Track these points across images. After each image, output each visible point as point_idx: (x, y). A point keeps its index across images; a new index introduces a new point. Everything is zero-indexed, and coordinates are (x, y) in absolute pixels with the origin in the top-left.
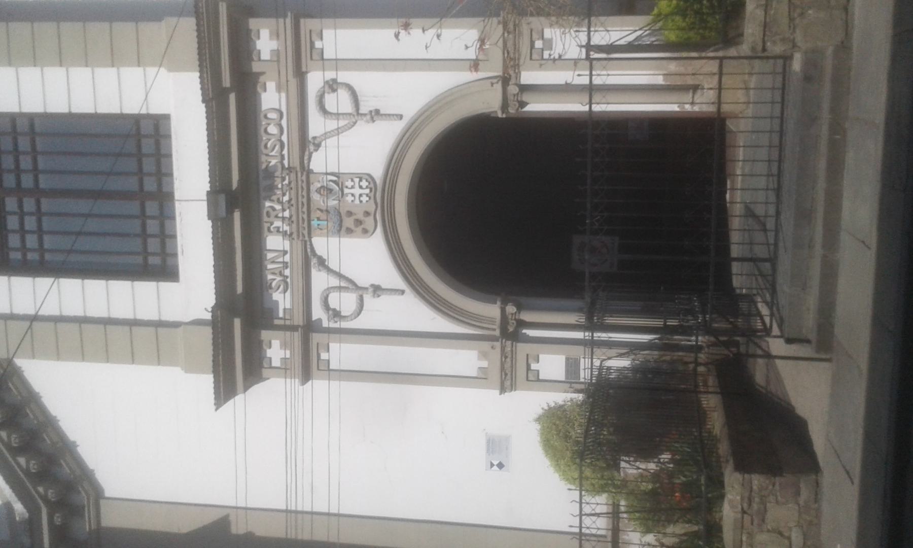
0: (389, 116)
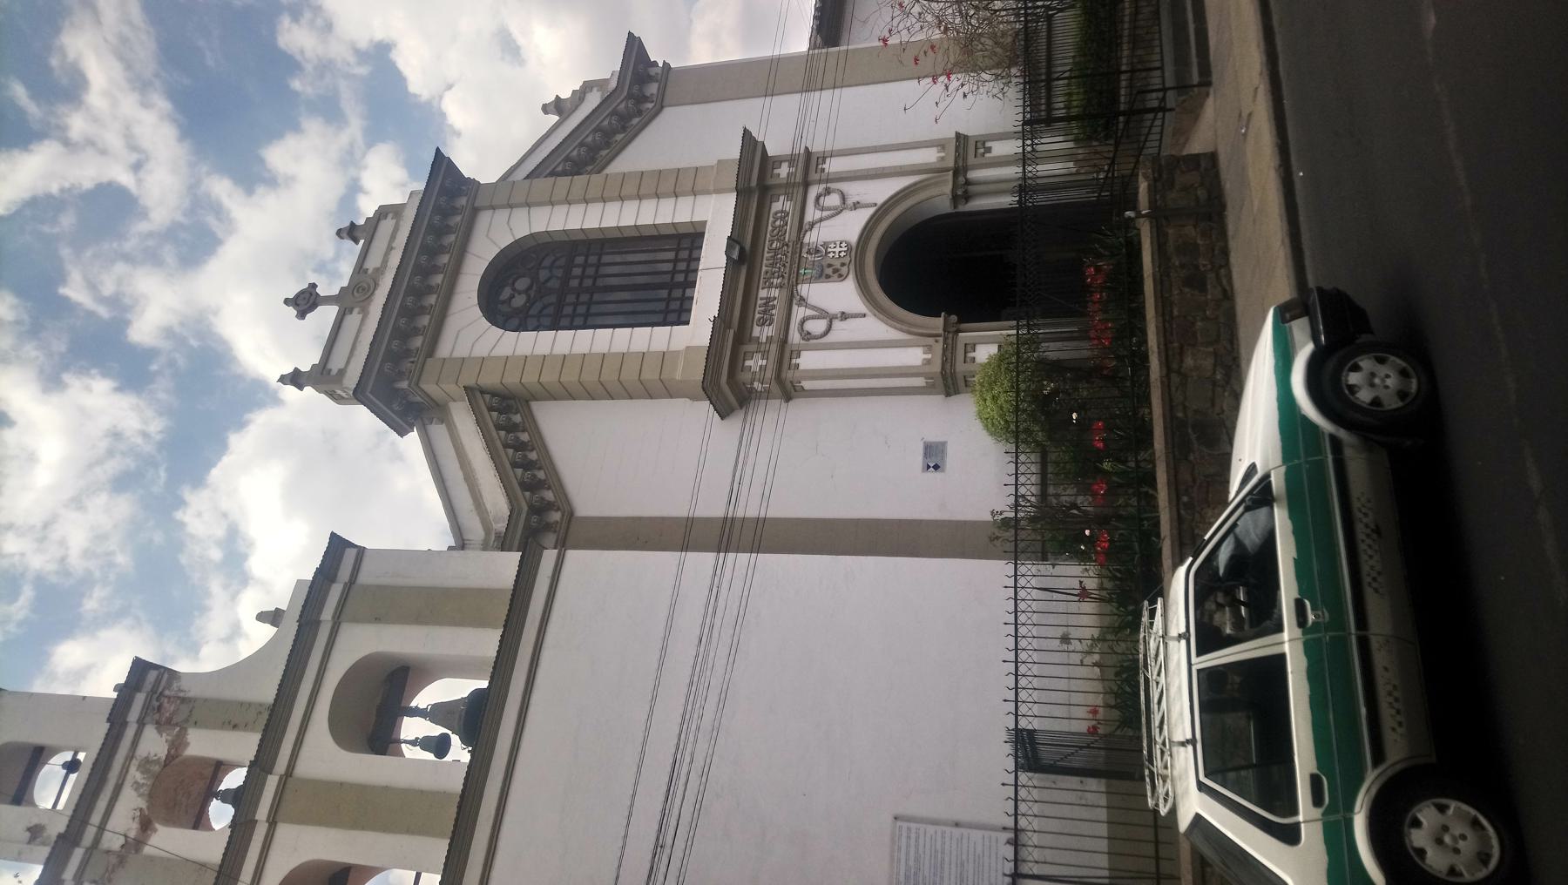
0: (867, 206)
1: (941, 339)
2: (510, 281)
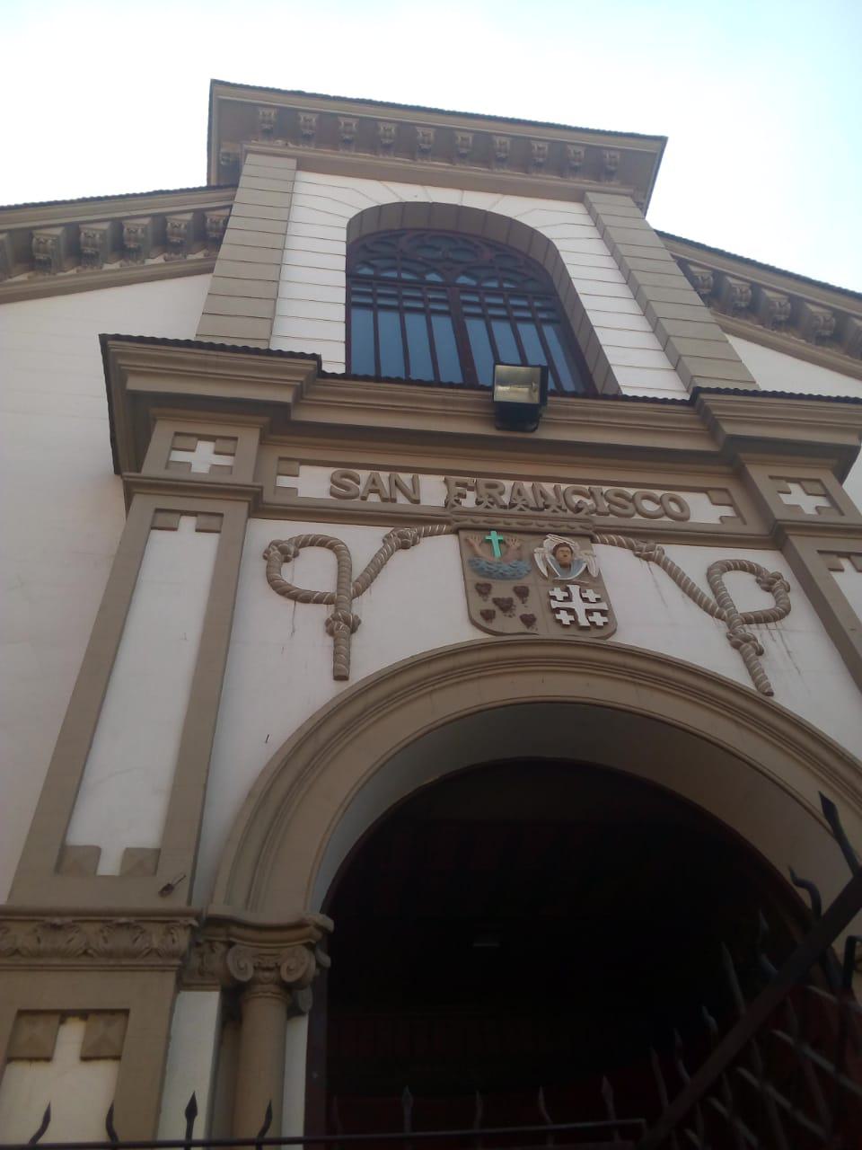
1: (177, 902)
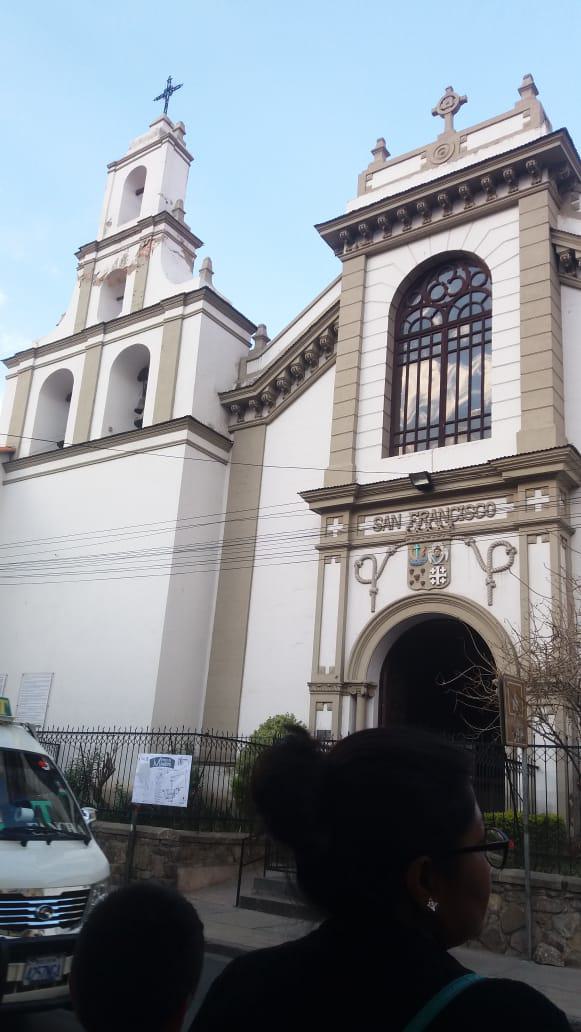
1: (338, 681)
2: (461, 272)
